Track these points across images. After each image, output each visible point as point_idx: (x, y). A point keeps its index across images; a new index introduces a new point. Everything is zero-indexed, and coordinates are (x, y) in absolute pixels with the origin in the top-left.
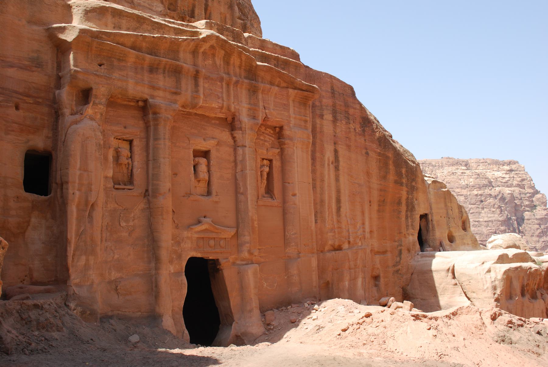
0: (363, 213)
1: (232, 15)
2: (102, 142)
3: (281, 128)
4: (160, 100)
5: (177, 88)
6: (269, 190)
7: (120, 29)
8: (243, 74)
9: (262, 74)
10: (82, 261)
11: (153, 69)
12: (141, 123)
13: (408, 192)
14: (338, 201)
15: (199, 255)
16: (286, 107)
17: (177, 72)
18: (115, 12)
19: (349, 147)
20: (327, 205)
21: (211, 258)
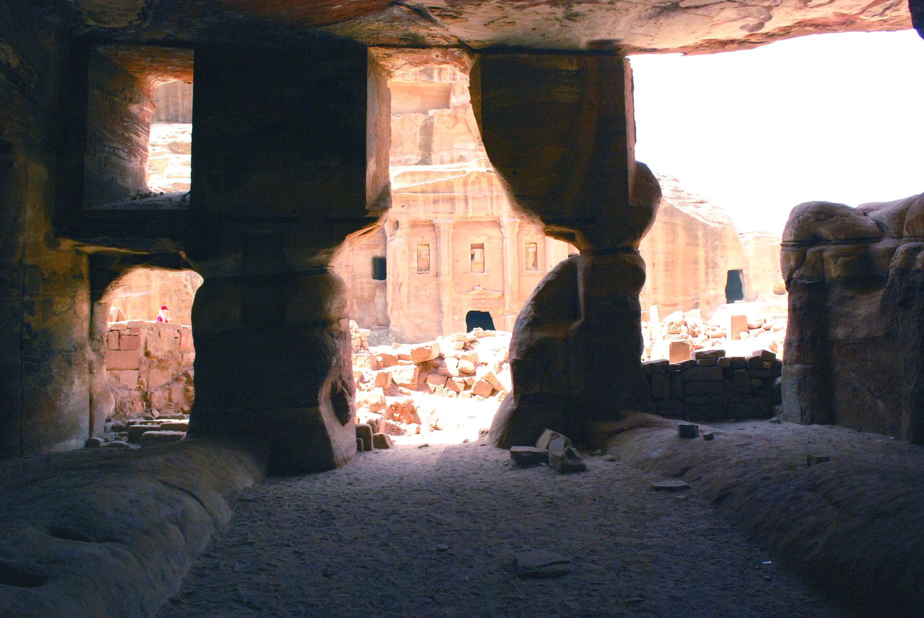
2: (407, 250)
4: (440, 220)
6: (535, 265)
10: (396, 313)
11: (435, 202)
13: (706, 252)
17: (452, 200)
18: (412, 174)
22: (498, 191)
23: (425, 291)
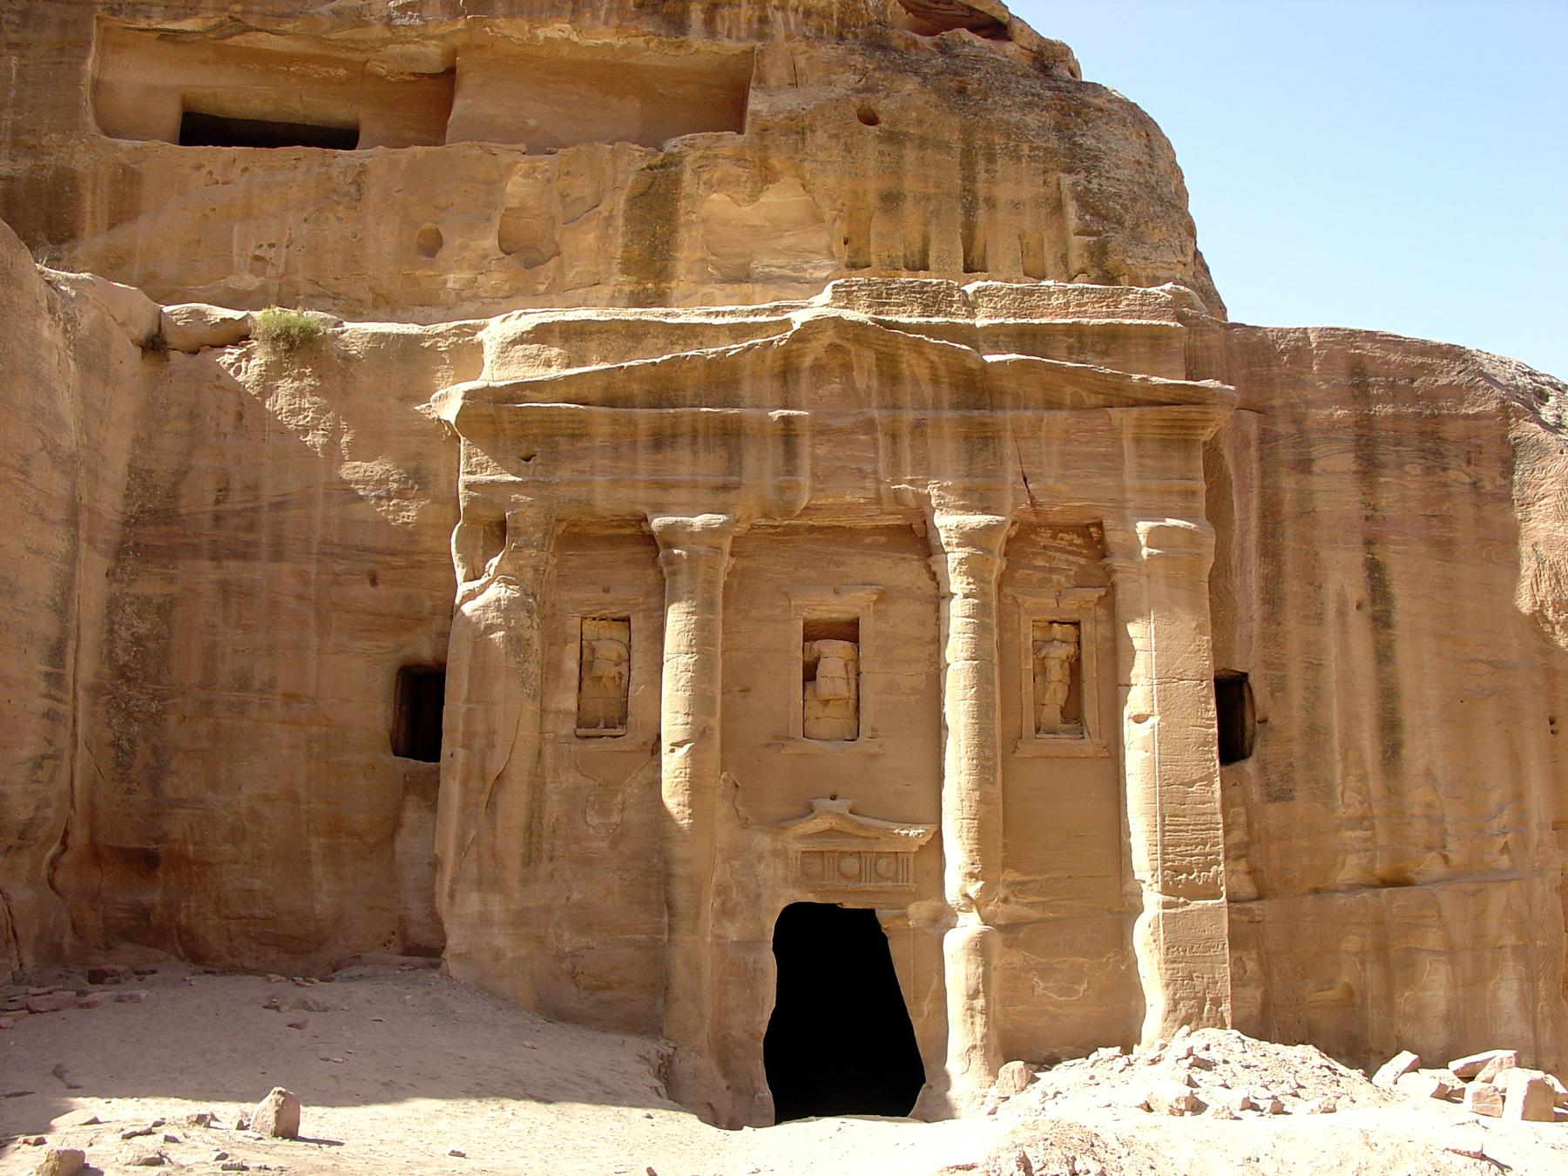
0: (1515, 760)
1: (1062, 228)
2: (535, 636)
3: (1100, 525)
5: (731, 474)
6: (1072, 713)
7: (584, 364)
8: (946, 396)
9: (1010, 385)
10: (471, 903)
11: (660, 440)
12: (651, 571)
14: (1390, 728)
15: (811, 898)
16: (1111, 463)
17: (729, 435)
19: (1444, 548)
20: (1336, 740)
21: (848, 906)
22: (920, 405)
23: (605, 812)
